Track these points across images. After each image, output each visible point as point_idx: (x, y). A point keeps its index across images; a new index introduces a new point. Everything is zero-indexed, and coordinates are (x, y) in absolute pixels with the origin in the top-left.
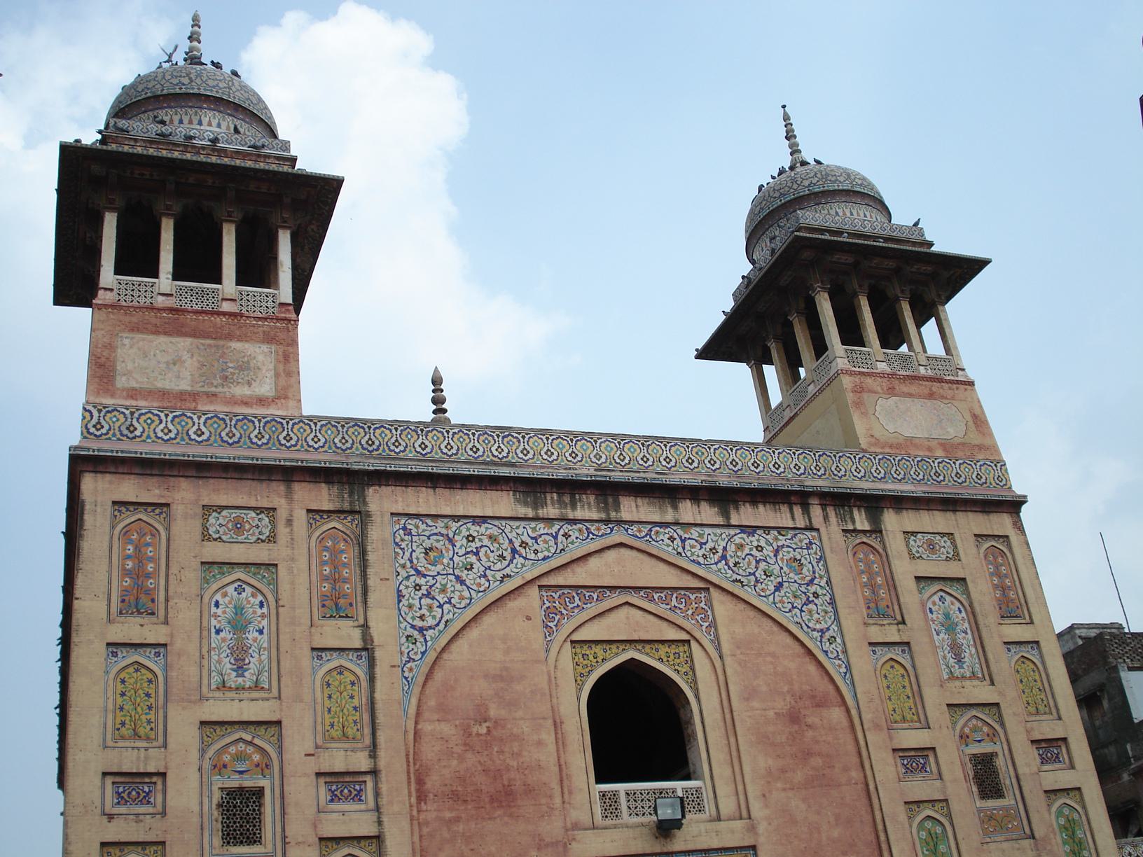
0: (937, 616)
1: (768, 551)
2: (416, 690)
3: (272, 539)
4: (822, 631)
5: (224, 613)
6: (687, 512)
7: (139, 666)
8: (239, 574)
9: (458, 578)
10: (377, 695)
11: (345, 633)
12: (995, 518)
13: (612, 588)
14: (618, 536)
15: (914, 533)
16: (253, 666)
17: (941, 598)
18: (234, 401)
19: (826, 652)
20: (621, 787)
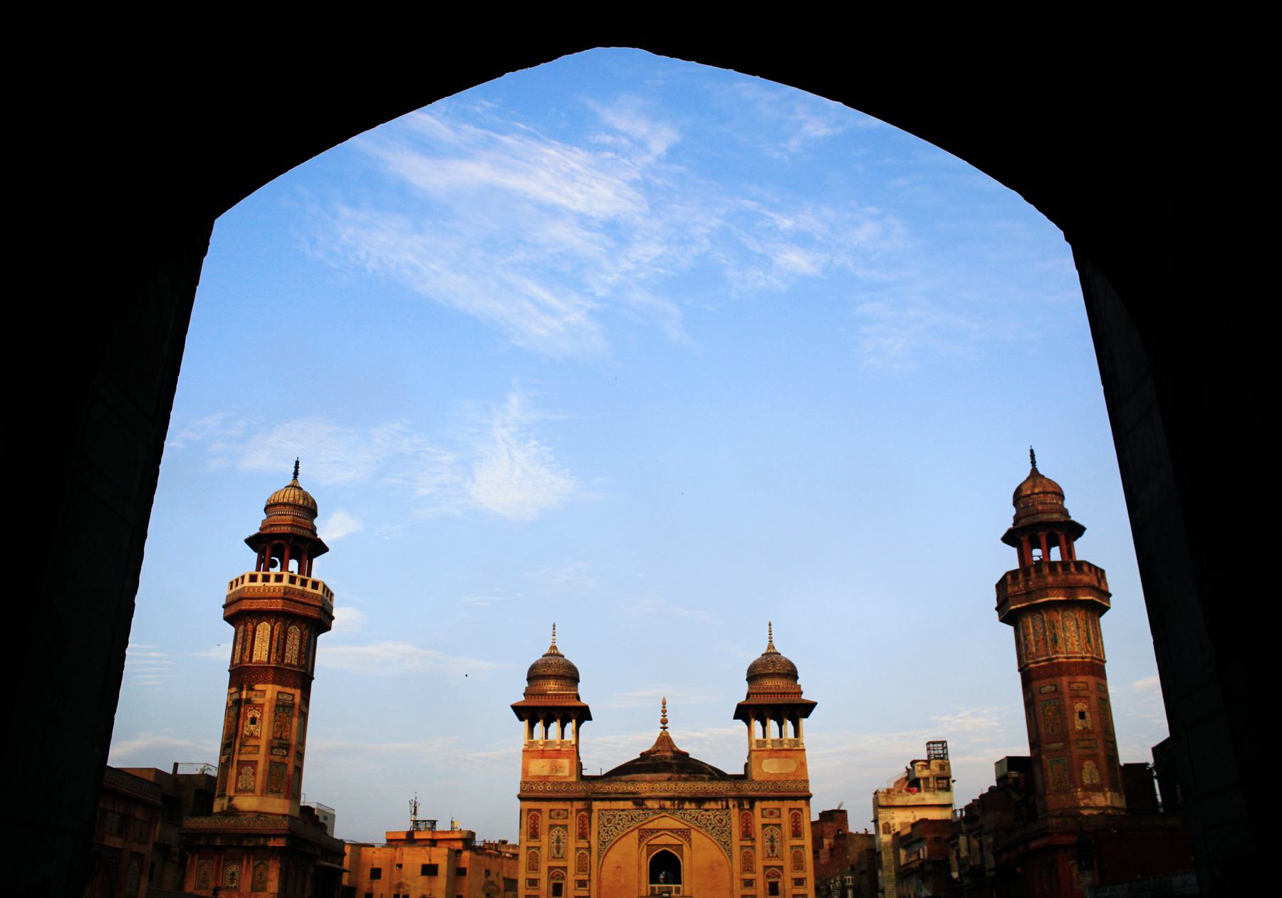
0: (768, 836)
1: (712, 817)
2: (602, 858)
3: (567, 818)
4: (725, 842)
5: (555, 838)
6: (687, 805)
7: (534, 852)
8: (558, 828)
9: (616, 828)
10: (592, 860)
11: (584, 844)
12: (799, 802)
13: (661, 829)
14: (663, 814)
15: (766, 809)
16: (561, 851)
17: (771, 831)
18: (558, 777)
19: (725, 849)
20: (657, 886)
